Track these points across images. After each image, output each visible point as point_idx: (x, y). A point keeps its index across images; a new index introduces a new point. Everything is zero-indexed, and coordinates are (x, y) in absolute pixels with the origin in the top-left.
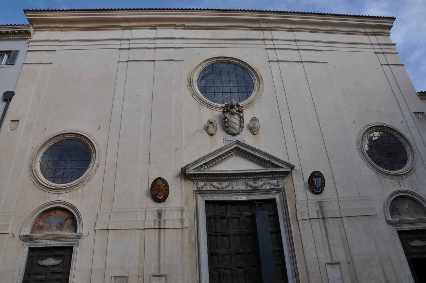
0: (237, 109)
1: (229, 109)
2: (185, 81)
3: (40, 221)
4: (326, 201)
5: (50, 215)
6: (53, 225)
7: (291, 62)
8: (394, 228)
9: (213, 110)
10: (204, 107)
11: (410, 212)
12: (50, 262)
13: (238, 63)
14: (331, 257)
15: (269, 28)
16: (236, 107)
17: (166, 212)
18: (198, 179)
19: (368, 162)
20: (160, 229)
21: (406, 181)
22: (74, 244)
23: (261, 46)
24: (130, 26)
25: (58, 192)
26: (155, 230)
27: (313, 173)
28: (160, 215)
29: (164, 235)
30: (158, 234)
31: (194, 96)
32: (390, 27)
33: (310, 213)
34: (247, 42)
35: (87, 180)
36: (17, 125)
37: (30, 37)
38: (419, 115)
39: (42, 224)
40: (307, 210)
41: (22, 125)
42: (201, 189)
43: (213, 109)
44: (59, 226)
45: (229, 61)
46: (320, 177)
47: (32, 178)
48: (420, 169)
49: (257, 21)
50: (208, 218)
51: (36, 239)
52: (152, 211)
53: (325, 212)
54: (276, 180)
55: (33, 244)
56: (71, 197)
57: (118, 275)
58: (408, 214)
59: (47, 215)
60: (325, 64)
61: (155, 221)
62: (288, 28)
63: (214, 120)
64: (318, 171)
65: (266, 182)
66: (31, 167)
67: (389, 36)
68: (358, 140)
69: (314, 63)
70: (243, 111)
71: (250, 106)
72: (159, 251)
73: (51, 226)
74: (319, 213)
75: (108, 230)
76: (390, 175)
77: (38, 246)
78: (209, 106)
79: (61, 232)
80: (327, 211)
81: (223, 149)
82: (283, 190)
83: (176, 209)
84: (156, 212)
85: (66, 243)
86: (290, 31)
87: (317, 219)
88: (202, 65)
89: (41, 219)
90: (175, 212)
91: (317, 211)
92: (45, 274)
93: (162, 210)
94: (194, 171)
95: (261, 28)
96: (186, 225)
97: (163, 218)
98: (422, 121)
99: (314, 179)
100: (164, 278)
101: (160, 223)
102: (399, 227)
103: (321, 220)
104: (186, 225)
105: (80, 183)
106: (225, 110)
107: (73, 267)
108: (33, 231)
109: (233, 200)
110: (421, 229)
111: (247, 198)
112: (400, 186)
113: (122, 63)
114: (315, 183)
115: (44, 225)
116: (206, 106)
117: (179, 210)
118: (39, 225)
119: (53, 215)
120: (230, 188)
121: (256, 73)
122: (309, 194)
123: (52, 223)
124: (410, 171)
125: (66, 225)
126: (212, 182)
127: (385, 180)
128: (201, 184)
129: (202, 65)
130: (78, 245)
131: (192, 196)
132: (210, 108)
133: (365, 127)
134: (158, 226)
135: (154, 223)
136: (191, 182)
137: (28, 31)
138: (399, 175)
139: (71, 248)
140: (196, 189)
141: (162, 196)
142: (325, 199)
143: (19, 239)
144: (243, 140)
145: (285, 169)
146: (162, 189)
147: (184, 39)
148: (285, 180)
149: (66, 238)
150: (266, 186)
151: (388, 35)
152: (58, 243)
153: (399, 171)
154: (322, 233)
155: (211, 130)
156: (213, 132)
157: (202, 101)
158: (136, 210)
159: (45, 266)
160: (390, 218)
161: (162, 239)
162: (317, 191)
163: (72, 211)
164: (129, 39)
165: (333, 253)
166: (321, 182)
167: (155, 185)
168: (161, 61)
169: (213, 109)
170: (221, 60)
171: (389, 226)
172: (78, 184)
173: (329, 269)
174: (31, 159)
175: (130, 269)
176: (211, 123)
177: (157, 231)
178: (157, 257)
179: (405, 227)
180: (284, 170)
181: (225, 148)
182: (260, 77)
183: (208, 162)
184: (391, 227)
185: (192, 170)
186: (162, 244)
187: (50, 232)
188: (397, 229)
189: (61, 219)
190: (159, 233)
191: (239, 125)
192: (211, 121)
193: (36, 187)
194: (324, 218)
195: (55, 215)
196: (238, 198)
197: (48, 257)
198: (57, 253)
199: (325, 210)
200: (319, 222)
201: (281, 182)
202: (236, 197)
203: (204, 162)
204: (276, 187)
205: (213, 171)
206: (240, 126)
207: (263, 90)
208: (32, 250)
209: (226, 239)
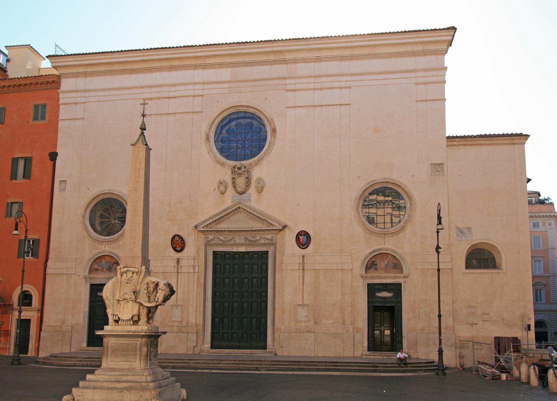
1: (236, 170)
2: (203, 136)
3: (95, 265)
4: (309, 256)
6: (104, 268)
11: (387, 268)
27: (300, 232)
39: (97, 267)
42: (210, 242)
44: (108, 268)
46: (306, 235)
53: (306, 264)
54: (271, 236)
60: (347, 106)
61: (174, 266)
64: (304, 231)
65: (262, 237)
68: (356, 198)
71: (260, 163)
73: (103, 268)
74: (301, 265)
78: (223, 164)
80: (308, 264)
81: (228, 209)
88: (220, 117)
89: (96, 264)
97: (180, 264)
98: (438, 173)
99: (301, 237)
100: (180, 307)
101: (178, 269)
104: (197, 271)
105: (120, 236)
106: (234, 171)
111: (246, 250)
114: (301, 241)
115: (98, 268)
117: (192, 259)
119: (104, 261)
120: (232, 242)
123: (103, 267)
128: (211, 237)
131: (203, 248)
141: (180, 248)
142: (309, 253)
143: (83, 278)
146: (179, 243)
147: (204, 83)
150: (262, 240)
156: (223, 191)
162: (302, 246)
166: (307, 240)
167: (174, 240)
172: (119, 237)
173: (300, 308)
176: (221, 183)
180: (276, 228)
181: (229, 208)
183: (215, 221)
189: (109, 264)
190: (178, 276)
191: (245, 184)
192: (222, 181)
199: (306, 262)
203: (212, 221)
204: (270, 242)
205: (219, 228)
206: (246, 186)
207: (274, 145)
208: (92, 285)
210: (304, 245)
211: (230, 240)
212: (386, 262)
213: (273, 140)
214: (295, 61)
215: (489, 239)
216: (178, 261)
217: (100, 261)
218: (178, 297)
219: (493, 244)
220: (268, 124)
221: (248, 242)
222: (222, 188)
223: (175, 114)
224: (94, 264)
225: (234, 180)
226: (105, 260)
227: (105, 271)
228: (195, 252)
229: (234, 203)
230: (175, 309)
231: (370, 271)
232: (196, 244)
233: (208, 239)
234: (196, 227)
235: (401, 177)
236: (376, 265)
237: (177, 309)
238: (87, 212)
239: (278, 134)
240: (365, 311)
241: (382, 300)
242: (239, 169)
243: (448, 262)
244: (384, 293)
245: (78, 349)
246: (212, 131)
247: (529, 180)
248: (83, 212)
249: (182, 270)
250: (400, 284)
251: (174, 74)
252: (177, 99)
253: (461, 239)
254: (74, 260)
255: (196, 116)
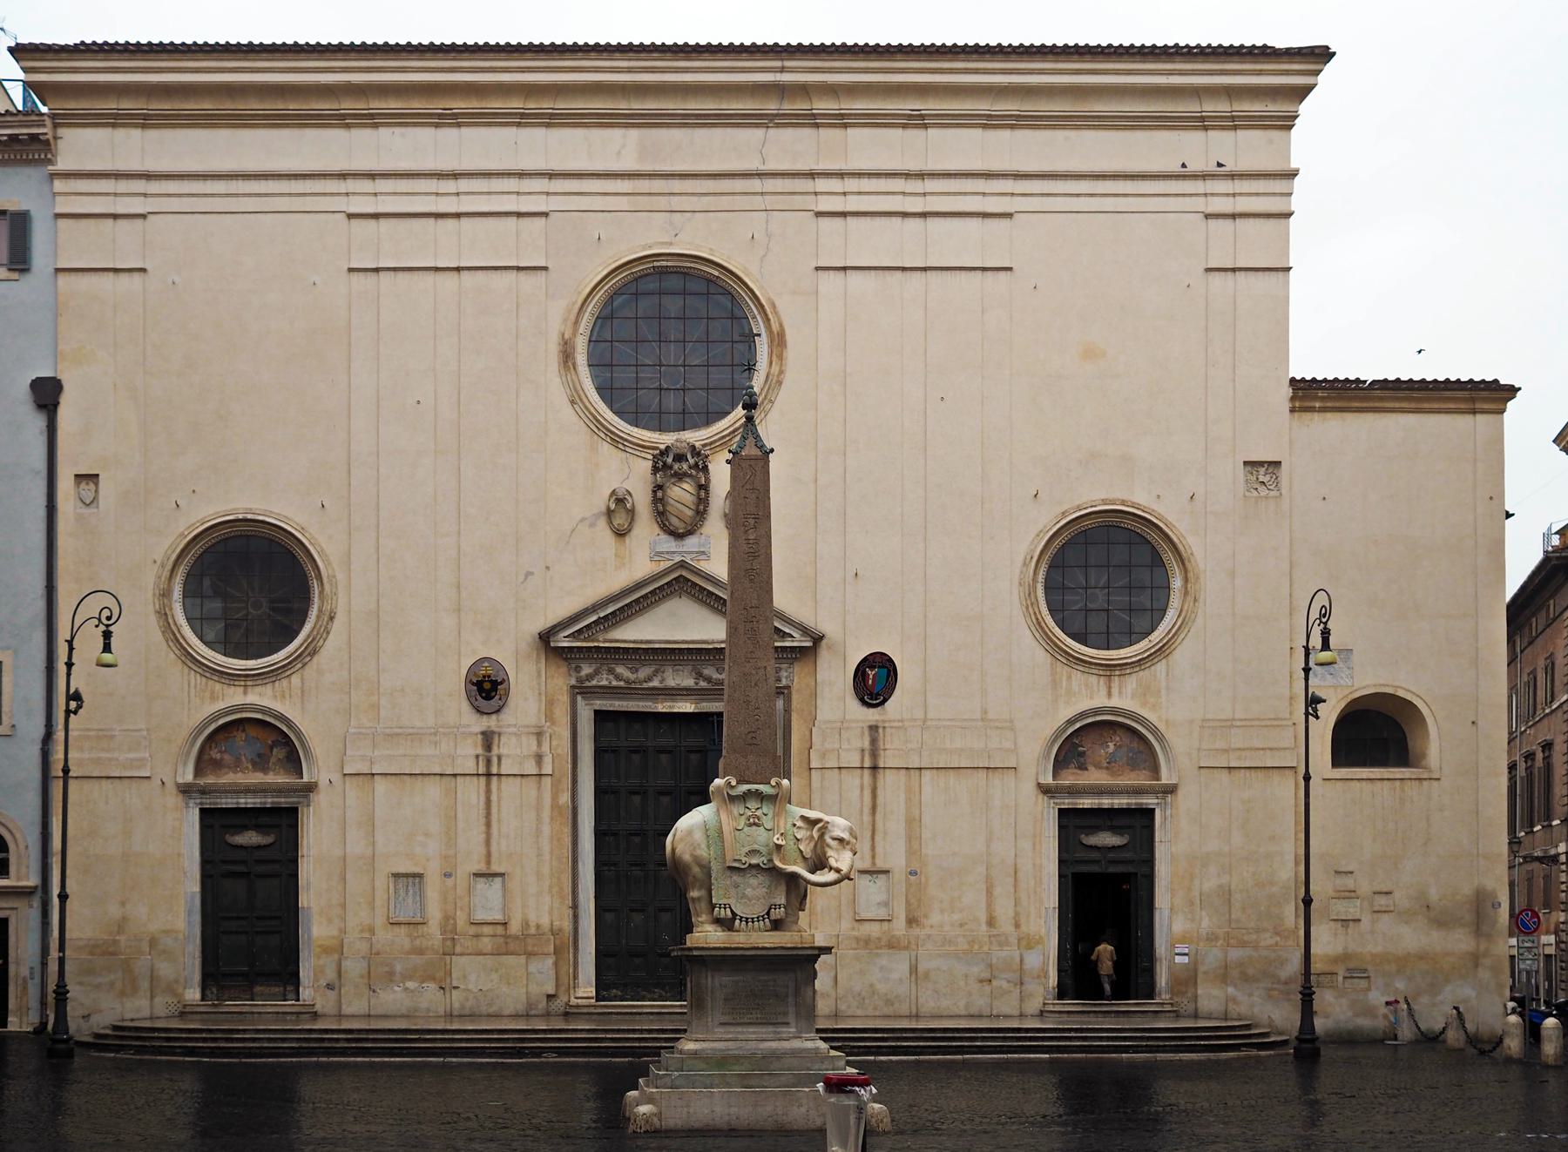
0: (692, 461)
2: (554, 348)
3: (211, 747)
4: (892, 727)
5: (232, 735)
7: (887, 273)
8: (1052, 801)
9: (628, 454)
10: (605, 442)
12: (250, 838)
13: (718, 277)
14: (873, 857)
15: (842, 116)
16: (689, 457)
17: (502, 738)
18: (580, 658)
19: (1039, 624)
20: (489, 775)
21: (1131, 682)
22: (299, 803)
23: (798, 201)
24: (372, 116)
25: (243, 683)
26: (478, 780)
28: (488, 747)
29: (499, 789)
30: (484, 787)
31: (575, 406)
32: (1303, 92)
33: (843, 754)
34: (756, 185)
35: (309, 654)
36: (96, 491)
37: (49, 156)
38: (1262, 470)
39: (218, 756)
40: (837, 746)
41: (108, 487)
42: (587, 684)
43: (627, 449)
44: (258, 760)
45: (691, 268)
47: (171, 644)
48: (1183, 654)
49: (804, 90)
50: (599, 753)
51: (215, 791)
52: (471, 734)
53: (882, 752)
55: (208, 801)
56: (277, 694)
57: (402, 870)
58: (1107, 768)
59: (226, 735)
60: (1002, 274)
61: (477, 757)
62: (910, 117)
63: (627, 491)
66: (164, 615)
67: (1290, 127)
68: (1029, 557)
69: (963, 273)
70: (710, 467)
72: (488, 825)
75: (373, 775)
76: (1091, 663)
77: (219, 806)
78: (617, 441)
79: (266, 774)
82: (786, 691)
83: (526, 730)
84: (480, 737)
85: (283, 800)
86: (916, 126)
87: (859, 770)
88: (606, 288)
89: (213, 745)
90: (524, 739)
91: (863, 750)
92: (244, 862)
93: (493, 733)
94: (568, 641)
95: (814, 116)
96: (547, 769)
97: (495, 751)
98: (1263, 491)
99: (870, 672)
100: (498, 880)
101: (489, 762)
102: (1066, 801)
103: (867, 772)
104: (547, 769)
107: (304, 850)
108: (199, 771)
109: (661, 711)
110: (1125, 807)
111: (695, 709)
112: (1109, 694)
113: (361, 274)
114: (870, 682)
115: (222, 759)
116: (609, 440)
117: (533, 733)
118: (211, 759)
119: (239, 737)
120: (655, 683)
121: (769, 320)
122: (853, 704)
123: (240, 754)
124: (1154, 656)
125: (273, 760)
126: (613, 666)
127: (1069, 677)
128: (587, 670)
129: (606, 288)
130: (308, 805)
131: (565, 698)
132: (620, 446)
133: (1064, 514)
134: (485, 769)
135: (475, 763)
136: (563, 663)
137: (41, 137)
138: (1115, 665)
139: (293, 812)
140: (573, 682)
143: (174, 791)
144: (702, 550)
145: (799, 640)
147: (552, 175)
148: (797, 668)
149: (280, 790)
151: (1286, 123)
152: (263, 800)
153: (1123, 652)
154: (862, 802)
155: (620, 520)
157: (598, 426)
158: (433, 730)
159: (241, 847)
160: (1048, 779)
161: (494, 798)
162: (871, 699)
163: (285, 729)
164: (372, 176)
165: (879, 849)
168: (480, 272)
169: (627, 449)
170: (664, 263)
171: (1041, 796)
172: (290, 663)
174: (157, 592)
175: (428, 860)
176: (620, 501)
177: (483, 780)
178: (484, 836)
179: (1081, 801)
180: (795, 644)
182: (778, 334)
184: (1043, 799)
185: (565, 637)
186: (494, 810)
187: (240, 774)
188: (1060, 804)
190: (488, 784)
193: (186, 670)
194: (874, 768)
195: (244, 735)
196: (673, 707)
197: (245, 828)
198: (263, 820)
199: (882, 747)
200: (862, 777)
201: (786, 671)
202: (668, 704)
203: (594, 618)
205: (617, 641)
206: (698, 512)
209: (637, 799)
210: (878, 694)
211: (650, 679)
212: (1111, 745)
213: (775, 369)
214: (842, 121)
215: (1397, 684)
216: (488, 739)
217: (229, 737)
218: (494, 848)
219: (1408, 697)
220: (758, 317)
221: (703, 684)
222: (620, 520)
223: (458, 269)
224: (207, 747)
225: (660, 494)
226: (244, 735)
227: (247, 768)
228: (539, 710)
229: (664, 565)
230: (483, 885)
231: (1064, 773)
232: (543, 688)
233: (579, 672)
234: (545, 637)
235: (1159, 497)
236: (1082, 754)
237: (491, 885)
238: (177, 581)
239: (791, 353)
240: (1052, 887)
241: (1095, 855)
242: (680, 458)
243: (1285, 749)
244: (1104, 835)
245: (176, 1008)
246: (581, 331)
247: (1509, 515)
248: (163, 579)
249: (503, 766)
250: (1150, 813)
251: (449, 134)
252: (464, 220)
253: (1322, 684)
254: (145, 733)
255: (527, 281)
